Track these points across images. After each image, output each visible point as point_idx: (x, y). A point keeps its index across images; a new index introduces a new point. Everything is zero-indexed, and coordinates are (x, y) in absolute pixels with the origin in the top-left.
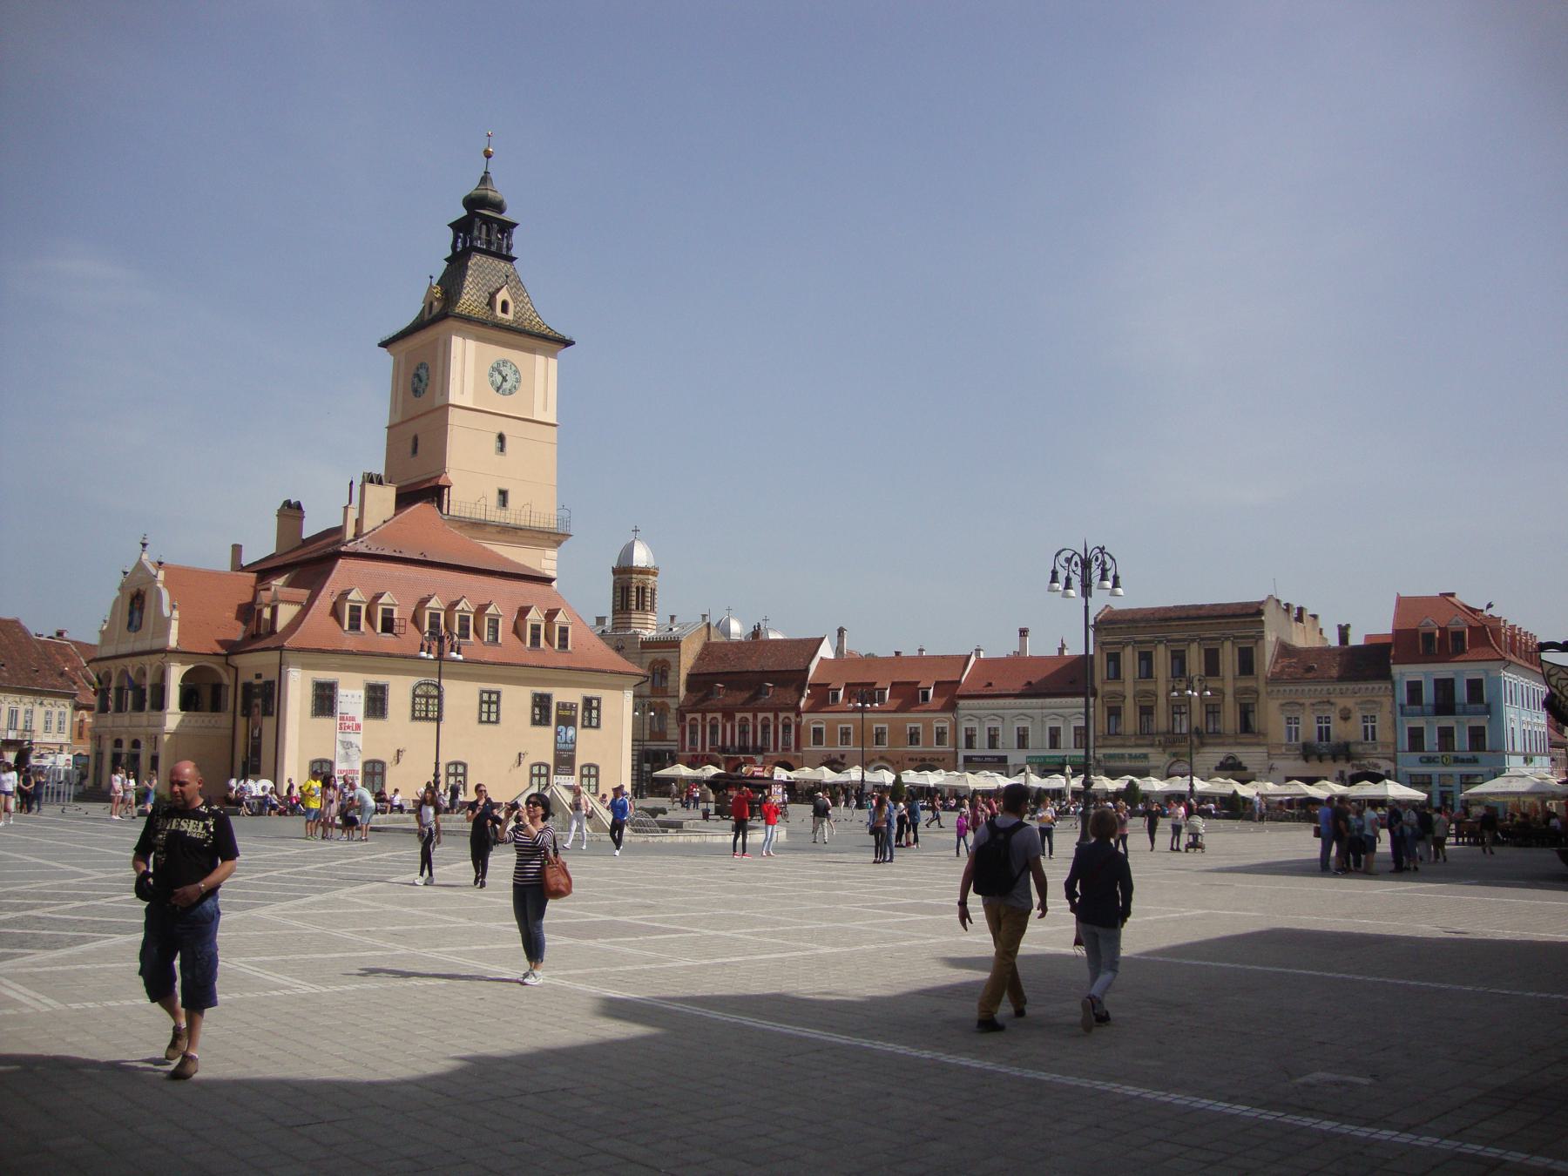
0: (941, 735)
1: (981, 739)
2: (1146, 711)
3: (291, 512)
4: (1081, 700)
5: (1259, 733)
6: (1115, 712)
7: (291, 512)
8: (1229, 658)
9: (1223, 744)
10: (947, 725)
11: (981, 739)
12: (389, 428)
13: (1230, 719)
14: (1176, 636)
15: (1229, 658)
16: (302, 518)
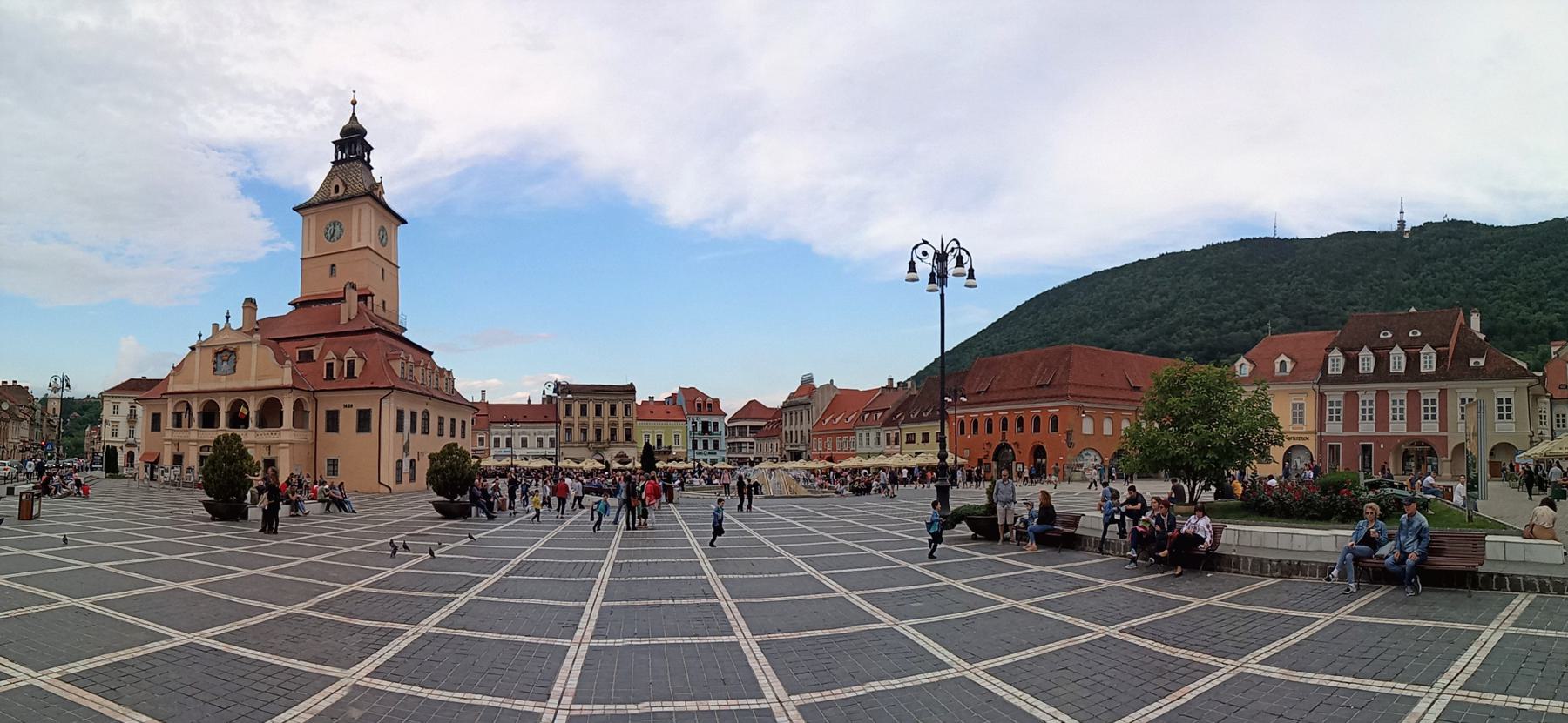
0: (481, 440)
1: (503, 442)
2: (584, 432)
3: (249, 304)
4: (554, 425)
5: (634, 442)
6: (569, 431)
7: (250, 304)
8: (620, 408)
9: (617, 446)
10: (484, 436)
11: (503, 442)
12: (302, 259)
13: (621, 435)
14: (597, 398)
15: (620, 408)
16: (256, 309)
